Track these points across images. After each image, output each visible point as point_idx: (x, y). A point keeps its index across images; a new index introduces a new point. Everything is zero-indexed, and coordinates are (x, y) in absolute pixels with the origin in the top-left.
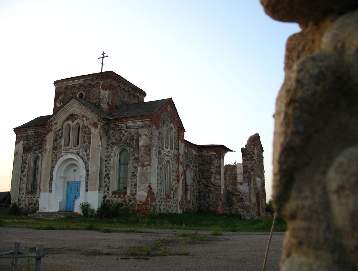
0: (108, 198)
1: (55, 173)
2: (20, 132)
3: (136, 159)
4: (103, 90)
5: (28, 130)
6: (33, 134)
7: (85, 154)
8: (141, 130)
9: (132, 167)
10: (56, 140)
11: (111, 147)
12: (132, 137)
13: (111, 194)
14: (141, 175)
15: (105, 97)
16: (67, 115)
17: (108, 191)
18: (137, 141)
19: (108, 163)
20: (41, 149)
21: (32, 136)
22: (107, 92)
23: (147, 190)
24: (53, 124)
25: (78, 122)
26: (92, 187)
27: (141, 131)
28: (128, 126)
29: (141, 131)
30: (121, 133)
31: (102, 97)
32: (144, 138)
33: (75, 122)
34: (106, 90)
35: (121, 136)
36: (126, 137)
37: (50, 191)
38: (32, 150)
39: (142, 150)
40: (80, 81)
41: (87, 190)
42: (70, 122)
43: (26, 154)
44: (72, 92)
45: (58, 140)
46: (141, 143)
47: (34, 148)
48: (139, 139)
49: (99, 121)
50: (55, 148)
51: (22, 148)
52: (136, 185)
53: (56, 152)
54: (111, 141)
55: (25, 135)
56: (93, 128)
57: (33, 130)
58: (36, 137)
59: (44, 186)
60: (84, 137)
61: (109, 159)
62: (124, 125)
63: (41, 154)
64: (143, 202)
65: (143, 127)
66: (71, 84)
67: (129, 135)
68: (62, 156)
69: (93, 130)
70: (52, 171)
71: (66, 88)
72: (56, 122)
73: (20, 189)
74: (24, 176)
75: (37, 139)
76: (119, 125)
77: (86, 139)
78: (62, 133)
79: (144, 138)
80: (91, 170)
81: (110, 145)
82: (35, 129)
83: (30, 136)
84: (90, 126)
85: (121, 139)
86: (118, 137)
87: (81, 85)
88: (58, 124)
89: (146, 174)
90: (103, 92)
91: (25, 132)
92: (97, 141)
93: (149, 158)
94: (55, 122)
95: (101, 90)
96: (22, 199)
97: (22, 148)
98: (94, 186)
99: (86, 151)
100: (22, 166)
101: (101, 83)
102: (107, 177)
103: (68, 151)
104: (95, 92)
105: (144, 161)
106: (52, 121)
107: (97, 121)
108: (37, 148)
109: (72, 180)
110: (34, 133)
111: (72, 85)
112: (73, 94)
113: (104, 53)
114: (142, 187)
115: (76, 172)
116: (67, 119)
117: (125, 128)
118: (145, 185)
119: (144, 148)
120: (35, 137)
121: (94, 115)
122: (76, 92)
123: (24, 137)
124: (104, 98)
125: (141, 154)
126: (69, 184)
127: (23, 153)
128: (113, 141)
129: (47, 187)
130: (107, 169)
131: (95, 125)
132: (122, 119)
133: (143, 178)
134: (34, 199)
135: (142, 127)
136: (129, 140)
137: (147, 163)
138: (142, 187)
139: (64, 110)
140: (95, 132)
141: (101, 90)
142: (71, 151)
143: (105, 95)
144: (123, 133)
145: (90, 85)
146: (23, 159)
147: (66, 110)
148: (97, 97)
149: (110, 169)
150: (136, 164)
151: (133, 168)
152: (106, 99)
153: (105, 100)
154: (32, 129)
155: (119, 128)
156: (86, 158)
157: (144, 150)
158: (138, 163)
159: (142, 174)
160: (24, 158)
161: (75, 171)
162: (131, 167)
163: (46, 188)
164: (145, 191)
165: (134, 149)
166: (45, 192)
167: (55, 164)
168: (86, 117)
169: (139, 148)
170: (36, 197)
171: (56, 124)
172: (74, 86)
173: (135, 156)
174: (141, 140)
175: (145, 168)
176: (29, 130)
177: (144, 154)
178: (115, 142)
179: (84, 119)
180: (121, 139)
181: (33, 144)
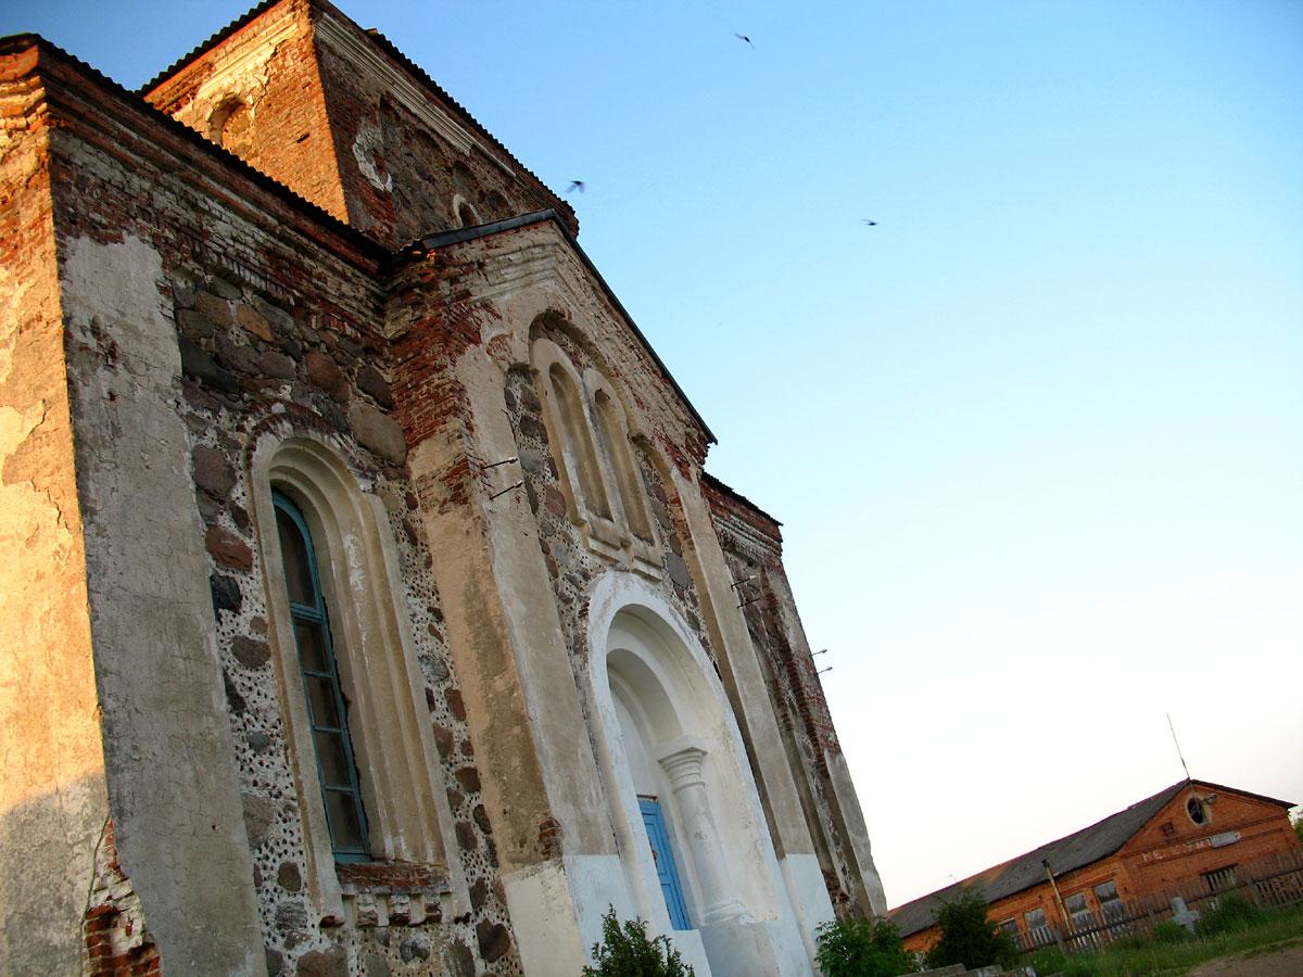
2: (125, 141)
5: (215, 185)
40: (461, 142)
43: (215, 413)
51: (158, 317)
57: (262, 226)
66: (414, 110)
73: (257, 823)
74: (251, 654)
82: (282, 220)
87: (462, 167)
96: (301, 951)
97: (168, 329)
111: (415, 116)
134: (421, 938)
154: (258, 203)
163: (589, 810)
166: (592, 852)
176: (225, 192)
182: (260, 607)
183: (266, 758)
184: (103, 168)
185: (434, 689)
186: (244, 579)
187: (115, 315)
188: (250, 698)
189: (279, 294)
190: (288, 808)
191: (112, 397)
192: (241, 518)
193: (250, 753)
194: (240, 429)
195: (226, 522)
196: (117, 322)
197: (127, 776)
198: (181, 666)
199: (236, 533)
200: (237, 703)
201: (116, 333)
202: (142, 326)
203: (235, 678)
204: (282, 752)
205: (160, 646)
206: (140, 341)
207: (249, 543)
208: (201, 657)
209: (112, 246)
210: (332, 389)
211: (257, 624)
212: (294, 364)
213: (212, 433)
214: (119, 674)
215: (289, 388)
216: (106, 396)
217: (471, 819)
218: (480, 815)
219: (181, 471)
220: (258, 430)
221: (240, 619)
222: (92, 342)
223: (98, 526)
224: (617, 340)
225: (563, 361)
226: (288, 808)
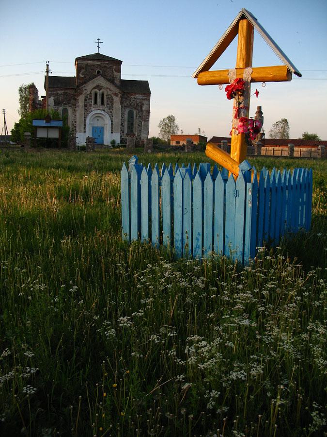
0: (123, 137)
1: (87, 121)
3: (140, 116)
10: (85, 100)
12: (137, 105)
13: (125, 135)
16: (95, 85)
18: (141, 108)
21: (61, 94)
24: (84, 89)
29: (144, 102)
30: (130, 101)
33: (101, 91)
37: (85, 132)
39: (145, 112)
41: (112, 133)
42: (97, 90)
46: (143, 109)
49: (119, 92)
50: (86, 106)
52: (141, 131)
55: (55, 93)
60: (108, 101)
62: (133, 97)
68: (92, 111)
69: (114, 97)
70: (85, 120)
71: (87, 65)
78: (91, 96)
81: (124, 107)
84: (112, 95)
85: (130, 105)
87: (99, 65)
92: (117, 105)
95: (114, 72)
97: (53, 102)
99: (109, 109)
101: (114, 67)
109: (96, 125)
112: (92, 70)
113: (99, 40)
114: (145, 133)
116: (93, 89)
123: (54, 94)
126: (93, 128)
131: (116, 95)
135: (144, 100)
138: (145, 133)
140: (117, 100)
141: (114, 72)
142: (99, 108)
145: (105, 66)
158: (142, 119)
159: (144, 126)
161: (98, 120)
168: (109, 89)
172: (93, 65)
175: (146, 122)
179: (109, 90)
180: (130, 105)
181: (62, 99)
210: (70, 100)
218: (76, 129)
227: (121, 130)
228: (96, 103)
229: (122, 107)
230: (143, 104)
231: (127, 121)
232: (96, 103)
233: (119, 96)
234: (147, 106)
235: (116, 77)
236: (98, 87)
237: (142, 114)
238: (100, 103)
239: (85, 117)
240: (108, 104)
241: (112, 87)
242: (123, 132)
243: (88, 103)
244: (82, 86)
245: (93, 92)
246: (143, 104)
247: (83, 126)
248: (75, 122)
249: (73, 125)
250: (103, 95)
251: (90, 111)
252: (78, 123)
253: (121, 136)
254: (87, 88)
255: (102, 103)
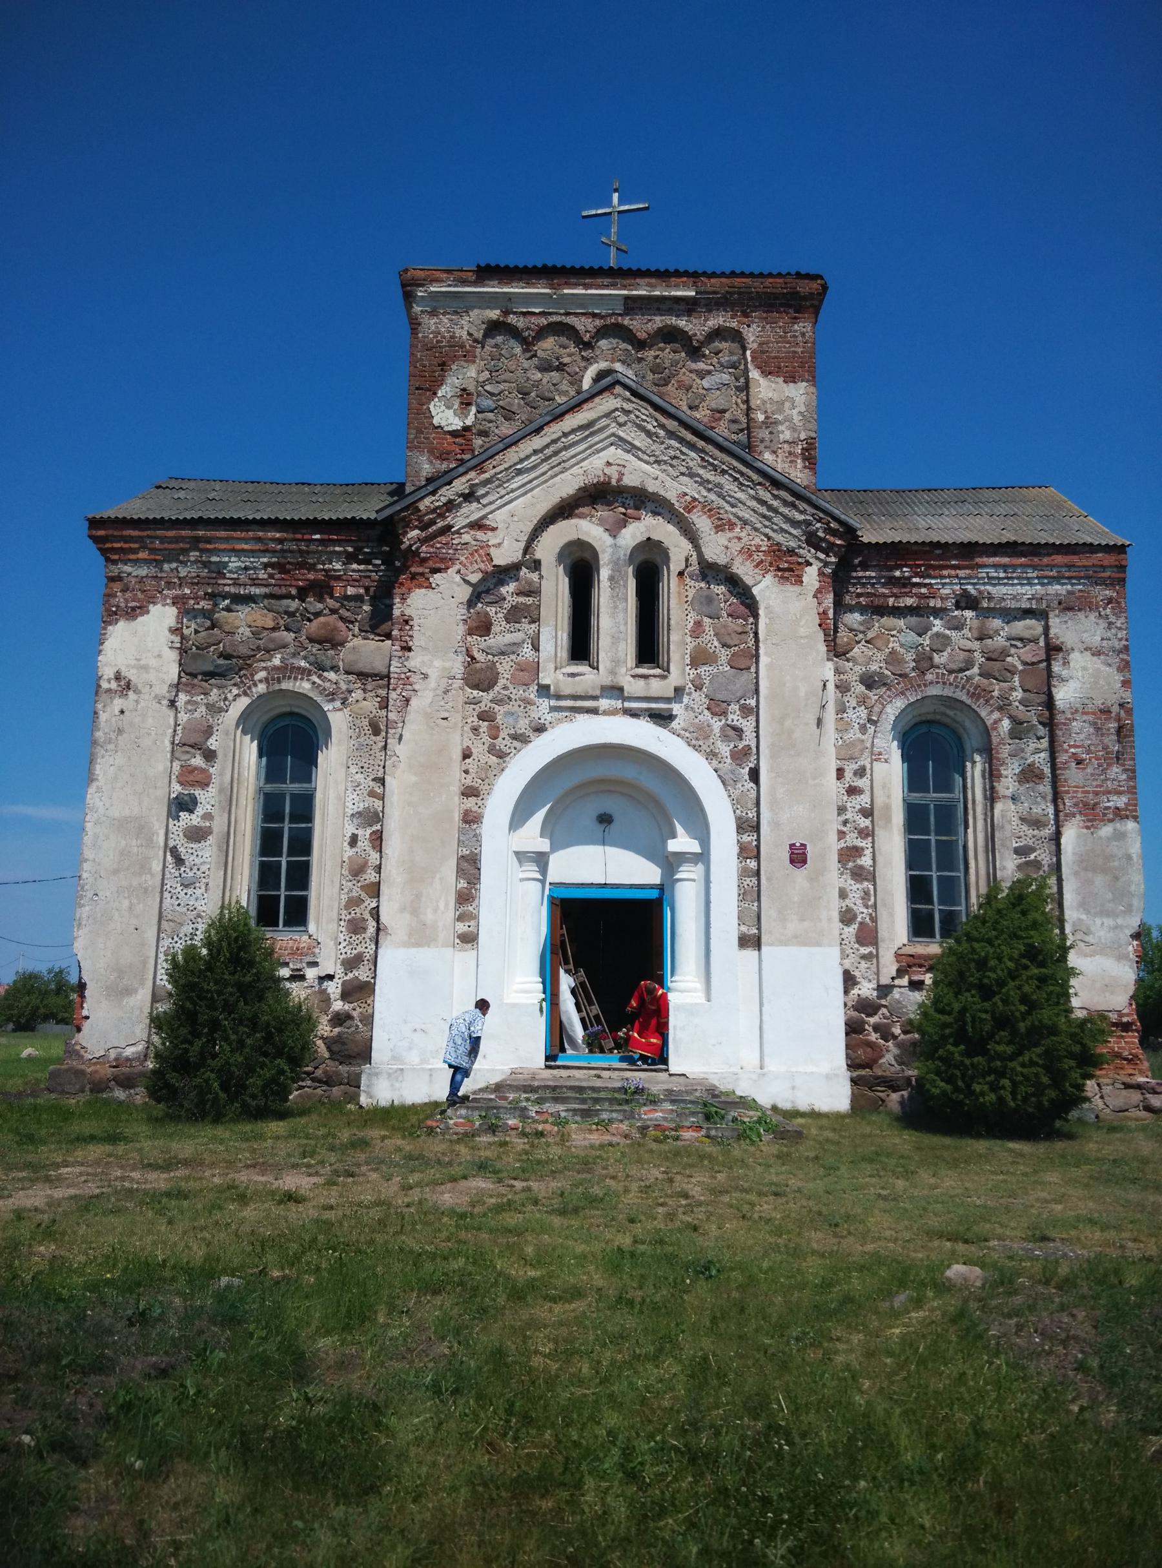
4: (766, 373)
6: (262, 575)
7: (717, 725)
8: (1057, 620)
9: (1016, 821)
11: (862, 701)
14: (1086, 869)
15: (788, 419)
16: (567, 484)
17: (865, 950)
19: (852, 791)
20: (332, 675)
22: (799, 394)
23: (1131, 948)
25: (655, 537)
26: (793, 926)
27: (1062, 628)
28: (973, 592)
29: (1062, 628)
31: (761, 417)
32: (1084, 669)
34: (791, 379)
35: (926, 641)
36: (963, 655)
38: (262, 674)
41: (751, 942)
44: (540, 353)
45: (495, 629)
46: (1064, 695)
47: (276, 661)
48: (1056, 668)
50: (480, 678)
53: (486, 697)
54: (859, 669)
56: (769, 580)
58: (288, 596)
59: (414, 909)
61: (856, 767)
63: (338, 704)
64: (1114, 1017)
65: (1070, 609)
67: (976, 645)
68: (540, 729)
69: (766, 588)
70: (471, 819)
72: (485, 517)
74: (197, 835)
75: (294, 605)
76: (915, 580)
77: (716, 643)
78: (533, 591)
79: (1084, 669)
80: (776, 825)
83: (236, 583)
85: (924, 662)
86: (902, 651)
88: (494, 529)
89: (1116, 864)
90: (765, 388)
91: (194, 555)
93: (1124, 777)
94: (470, 512)
95: (754, 374)
97: (174, 656)
98: (802, 920)
99: (717, 707)
100: (176, 766)
101: (752, 334)
102: (850, 865)
103: (581, 705)
104: (706, 383)
105: (1096, 793)
106: (450, 506)
107: (793, 544)
108: (303, 664)
110: (266, 566)
112: (545, 368)
115: (613, 826)
116: (564, 510)
117: (949, 604)
118: (1120, 921)
119: (1090, 718)
120: (277, 591)
121: (775, 503)
122: (566, 360)
124: (776, 423)
125: (1072, 750)
127: (177, 687)
128: (874, 667)
129: (435, 910)
130: (845, 823)
131: (786, 566)
132: (938, 552)
133: (1099, 880)
136: (976, 670)
137: (1121, 801)
139: (548, 452)
140: (790, 609)
141: (754, 374)
143: (787, 405)
144: (935, 629)
146: (176, 725)
147: (556, 453)
148: (724, 411)
149: (864, 822)
150: (1037, 803)
151: (1025, 828)
152: (794, 429)
153: (787, 435)
155: (909, 601)
156: (724, 749)
157: (1092, 730)
159: (1086, 863)
160: (183, 717)
162: (1009, 822)
163: (429, 916)
164: (1121, 958)
165: (1016, 722)
166: (418, 945)
167: (489, 775)
169: (1060, 718)
170: (311, 974)
171: (478, 525)
173: (1029, 761)
174: (1065, 673)
175: (1106, 830)
177: (1089, 752)
178: (886, 672)
182: (209, 807)
183: (190, 892)
184: (143, 571)
185: (360, 832)
186: (202, 792)
187: (133, 662)
188: (190, 860)
189: (284, 591)
190: (199, 916)
191: (122, 712)
192: (210, 755)
193: (179, 889)
194: (226, 699)
195: (198, 761)
196: (134, 667)
197: (87, 908)
198: (135, 850)
199: (204, 766)
200: (179, 861)
201: (131, 674)
202: (153, 662)
203: (181, 850)
204: (203, 887)
205: (124, 842)
206: (147, 672)
207: (212, 770)
208: (150, 843)
209: (140, 619)
210: (331, 641)
211: (208, 816)
212: (293, 635)
213: (203, 709)
214: (94, 860)
215: (279, 656)
216: (117, 713)
217: (367, 916)
218: (376, 913)
219: (163, 742)
220: (238, 695)
221: (193, 816)
222: (114, 685)
223: (98, 787)
224: (701, 471)
225: (587, 533)
226: (199, 916)
227: (847, 917)
228: (581, 647)
229: (843, 688)
230: (1053, 649)
231: (898, 817)
232: (581, 647)
233: (811, 575)
234: (1096, 663)
235: (769, 423)
236: (597, 495)
237: (1053, 751)
238: (628, 648)
239: (470, 792)
240: (699, 658)
241: (744, 500)
242: (868, 935)
243: (511, 649)
244: (447, 493)
245: (549, 546)
246: (1053, 649)
247: (448, 879)
248: (378, 840)
249: (357, 871)
250: (648, 571)
251: (523, 726)
252: (394, 845)
253: (849, 980)
254: (499, 518)
255: (649, 649)
